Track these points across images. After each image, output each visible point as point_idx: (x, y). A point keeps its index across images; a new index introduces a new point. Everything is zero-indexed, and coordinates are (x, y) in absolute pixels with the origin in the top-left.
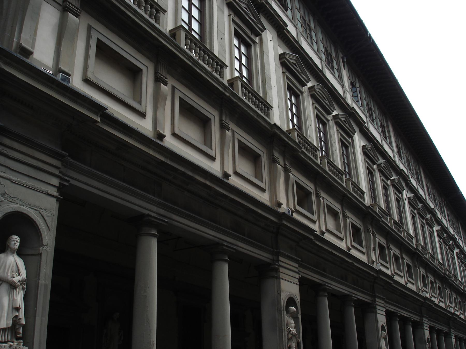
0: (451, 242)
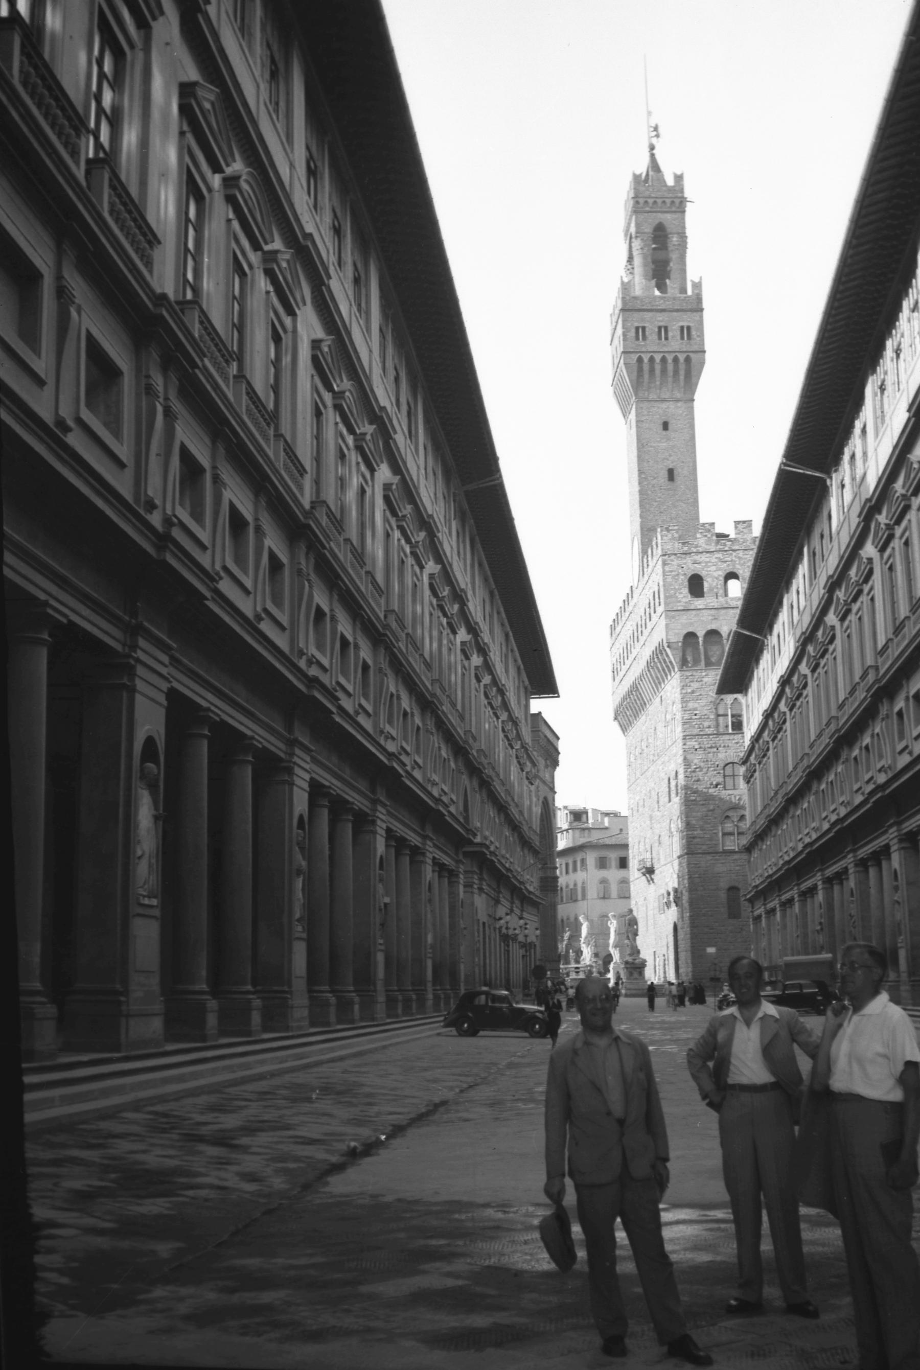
0: (423, 534)
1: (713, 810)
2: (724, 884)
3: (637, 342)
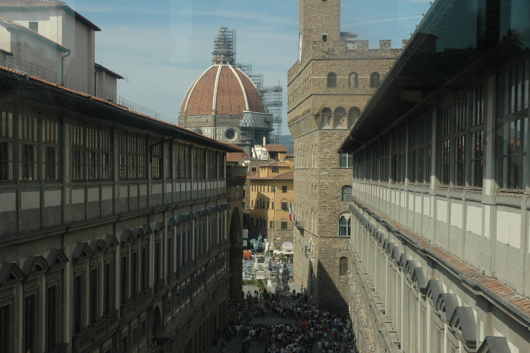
1: (335, 213)
2: (339, 255)
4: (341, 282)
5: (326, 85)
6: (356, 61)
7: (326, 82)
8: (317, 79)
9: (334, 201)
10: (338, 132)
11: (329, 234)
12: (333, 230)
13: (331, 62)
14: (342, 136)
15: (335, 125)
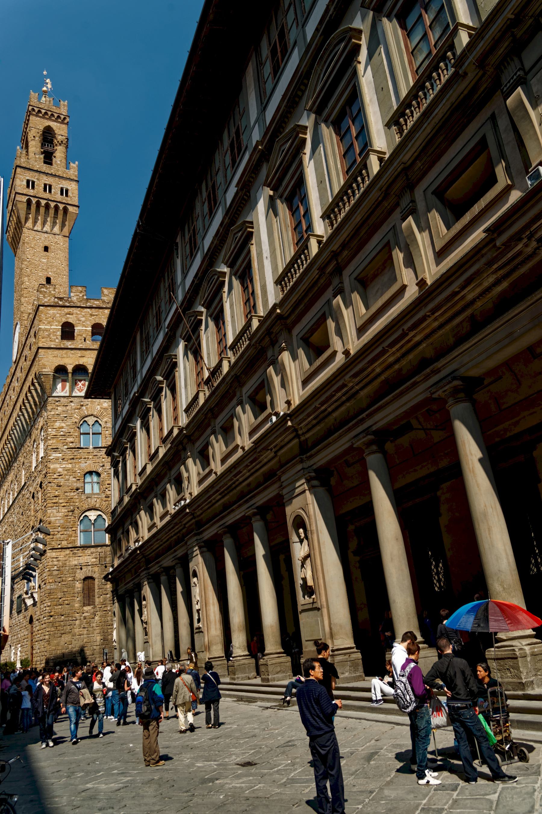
1: (73, 511)
2: (80, 575)
3: (27, 190)
4: (85, 618)
5: (60, 338)
6: (101, 310)
7: (59, 333)
8: (46, 330)
9: (72, 494)
10: (76, 400)
11: (64, 544)
12: (70, 536)
13: (66, 310)
14: (82, 406)
15: (72, 390)
